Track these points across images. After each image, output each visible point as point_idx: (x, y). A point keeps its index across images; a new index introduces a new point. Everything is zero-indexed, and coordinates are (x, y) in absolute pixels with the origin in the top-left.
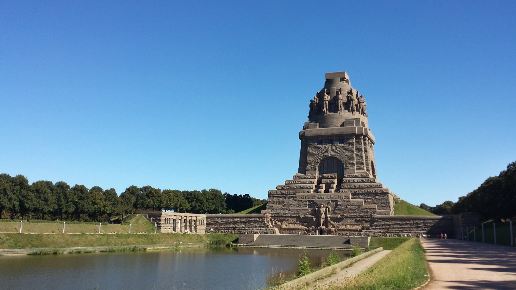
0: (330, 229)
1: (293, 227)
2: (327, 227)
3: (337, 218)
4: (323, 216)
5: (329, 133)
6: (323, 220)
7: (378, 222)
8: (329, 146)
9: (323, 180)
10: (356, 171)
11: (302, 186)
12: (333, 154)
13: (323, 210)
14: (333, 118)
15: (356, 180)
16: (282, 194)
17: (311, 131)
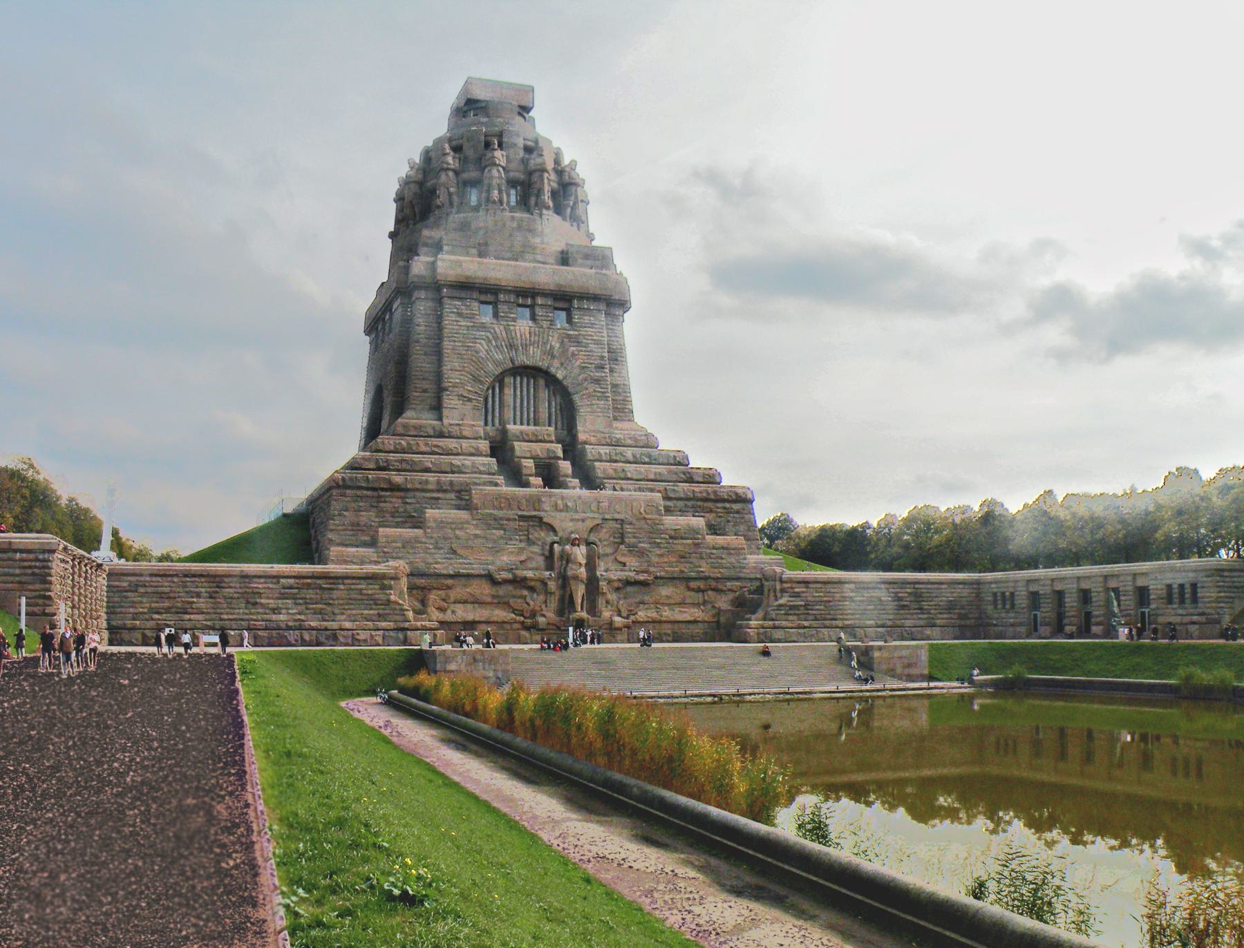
0: (611, 623)
1: (470, 617)
2: (593, 610)
3: (628, 583)
4: (582, 572)
5: (525, 281)
6: (580, 592)
7: (797, 595)
8: (523, 325)
9: (520, 448)
10: (615, 424)
11: (457, 461)
12: (534, 357)
13: (580, 553)
14: (530, 231)
15: (629, 453)
16: (394, 488)
17: (460, 264)
